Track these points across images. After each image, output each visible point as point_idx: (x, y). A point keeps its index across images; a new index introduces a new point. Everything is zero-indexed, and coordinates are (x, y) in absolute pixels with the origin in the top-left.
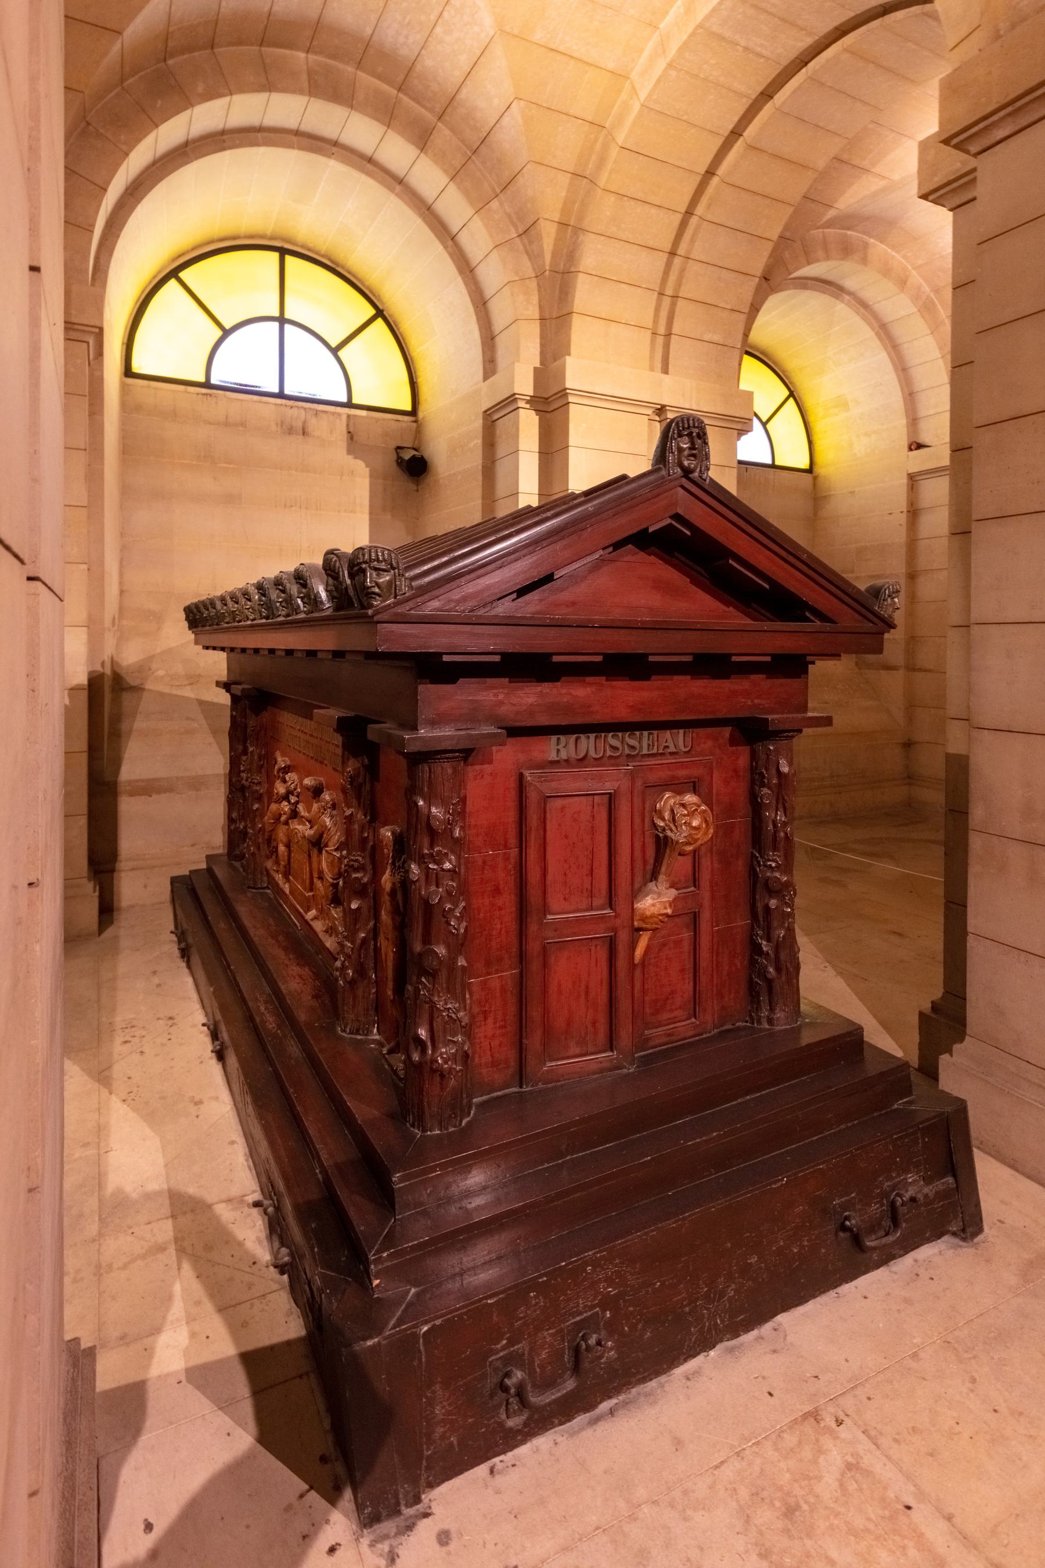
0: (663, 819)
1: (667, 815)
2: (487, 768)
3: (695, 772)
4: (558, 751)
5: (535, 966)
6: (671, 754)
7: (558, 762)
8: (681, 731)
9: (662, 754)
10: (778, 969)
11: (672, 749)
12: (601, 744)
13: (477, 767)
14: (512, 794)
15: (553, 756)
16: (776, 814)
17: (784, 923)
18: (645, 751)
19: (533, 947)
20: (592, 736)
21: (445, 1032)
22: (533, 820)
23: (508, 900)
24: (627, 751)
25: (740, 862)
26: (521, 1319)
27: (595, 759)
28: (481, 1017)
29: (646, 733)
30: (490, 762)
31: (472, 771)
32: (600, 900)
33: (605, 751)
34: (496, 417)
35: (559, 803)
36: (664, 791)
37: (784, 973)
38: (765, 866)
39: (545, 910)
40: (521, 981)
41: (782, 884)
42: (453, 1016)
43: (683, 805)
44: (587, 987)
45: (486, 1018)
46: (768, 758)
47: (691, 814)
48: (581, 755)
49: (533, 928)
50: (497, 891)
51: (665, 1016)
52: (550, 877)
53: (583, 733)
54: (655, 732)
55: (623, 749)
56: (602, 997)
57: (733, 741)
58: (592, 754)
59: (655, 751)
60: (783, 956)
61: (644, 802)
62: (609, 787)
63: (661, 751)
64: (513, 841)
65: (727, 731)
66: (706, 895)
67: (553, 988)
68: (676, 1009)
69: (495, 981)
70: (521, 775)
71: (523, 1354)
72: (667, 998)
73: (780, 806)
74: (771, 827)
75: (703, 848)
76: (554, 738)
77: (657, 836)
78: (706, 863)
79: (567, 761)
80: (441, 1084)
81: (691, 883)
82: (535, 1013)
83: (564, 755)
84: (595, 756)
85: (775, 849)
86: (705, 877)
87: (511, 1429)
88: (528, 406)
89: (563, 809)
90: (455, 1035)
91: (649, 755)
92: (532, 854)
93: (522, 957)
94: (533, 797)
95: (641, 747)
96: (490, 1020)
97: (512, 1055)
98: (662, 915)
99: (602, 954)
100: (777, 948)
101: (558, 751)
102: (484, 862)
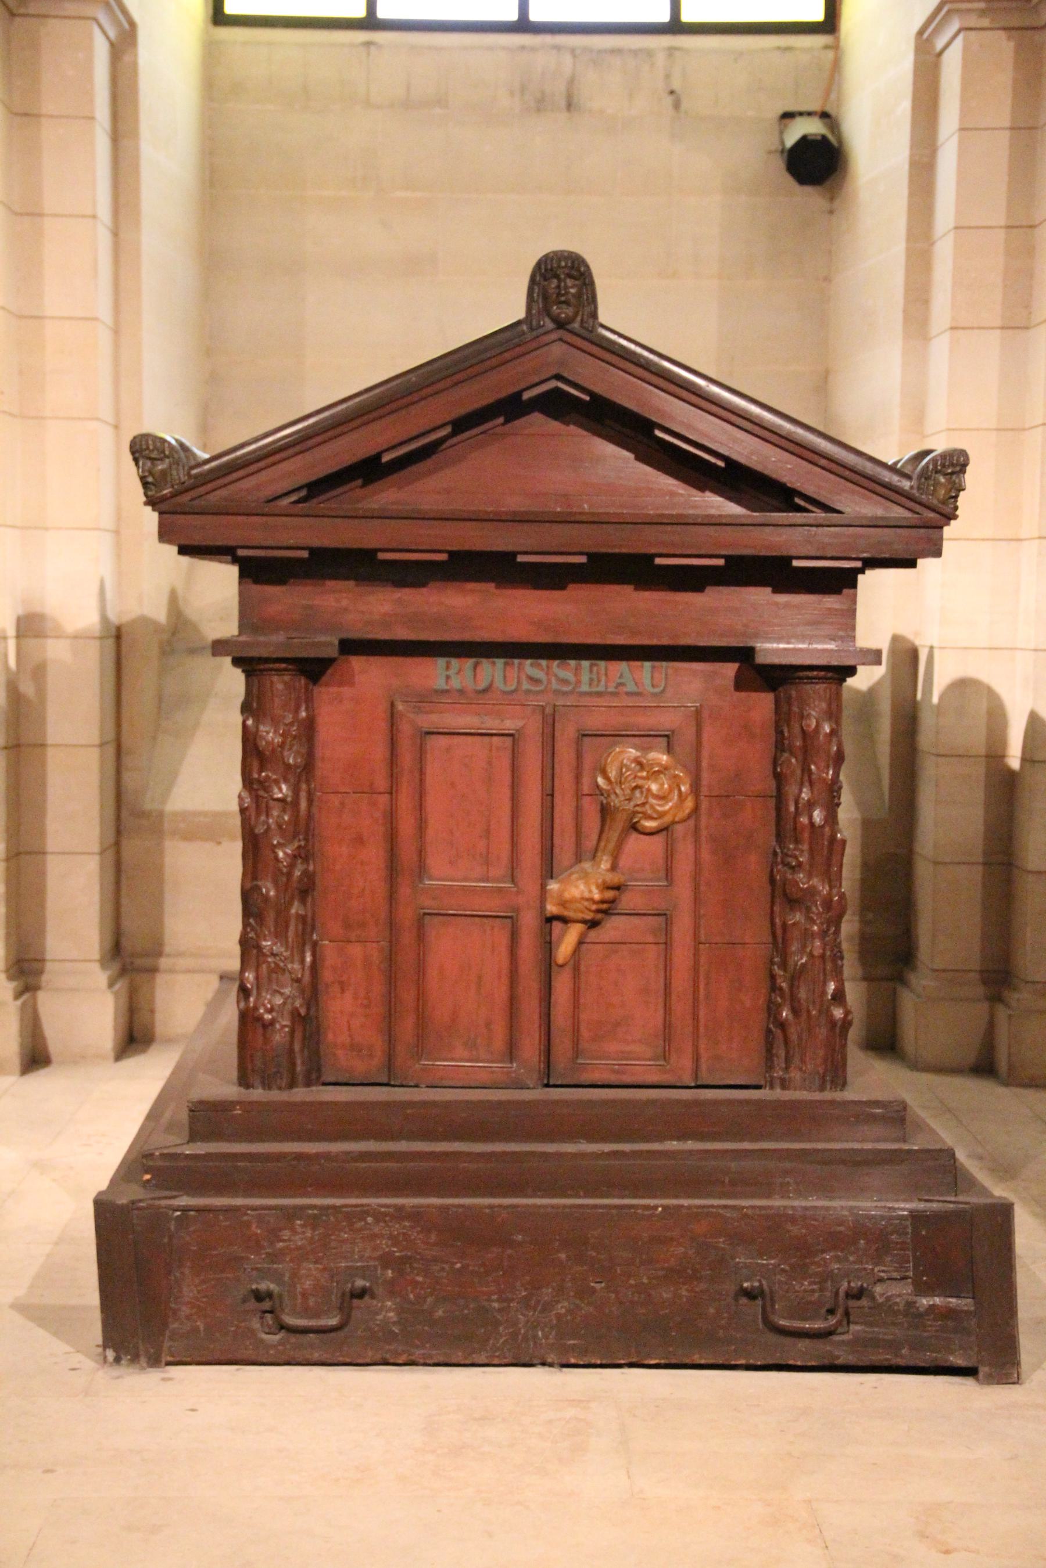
0: (607, 778)
1: (613, 774)
2: (346, 691)
3: (666, 720)
4: (448, 677)
5: (407, 938)
6: (627, 694)
7: (447, 691)
8: (647, 665)
9: (613, 694)
10: (795, 1012)
11: (631, 687)
12: (513, 673)
13: (333, 690)
14: (383, 726)
15: (440, 684)
16: (801, 791)
17: (804, 947)
18: (585, 688)
19: (406, 915)
20: (500, 662)
21: (270, 980)
22: (407, 759)
23: (374, 854)
24: (555, 685)
25: (753, 858)
26: (284, 1241)
27: (504, 693)
28: (336, 988)
29: (585, 664)
30: (351, 683)
31: (324, 693)
32: (500, 869)
33: (519, 682)
34: (940, 44)
35: (443, 741)
36: (615, 744)
37: (804, 1016)
38: (783, 863)
39: (421, 869)
40: (391, 958)
41: (802, 889)
42: (282, 964)
43: (640, 764)
44: (480, 977)
45: (343, 991)
46: (790, 709)
47: (654, 775)
48: (482, 685)
49: (404, 891)
50: (359, 840)
51: (612, 1047)
52: (430, 833)
53: (487, 656)
54: (602, 664)
55: (549, 682)
56: (501, 993)
57: (740, 685)
58: (499, 683)
59: (601, 688)
60: (802, 994)
61: (579, 756)
62: (510, 725)
63: (610, 690)
64: (381, 782)
65: (730, 669)
66: (683, 891)
67: (432, 973)
68: (634, 1041)
69: (356, 951)
70: (392, 705)
71: (283, 1275)
72: (618, 1024)
73: (806, 778)
74: (792, 809)
75: (679, 829)
76: (441, 662)
77: (602, 804)
78: (685, 851)
79: (461, 692)
80: (264, 1035)
81: (663, 874)
82: (408, 996)
83: (456, 683)
84: (502, 686)
85: (797, 841)
86: (684, 867)
87: (262, 1341)
88: (986, 22)
89: (448, 749)
90: (283, 987)
91: (590, 694)
92: (405, 800)
93: (392, 925)
94: (405, 728)
95: (579, 682)
96: (348, 996)
97: (379, 1044)
98: (587, 900)
99: (502, 939)
100: (794, 979)
101: (448, 677)
102: (342, 804)
